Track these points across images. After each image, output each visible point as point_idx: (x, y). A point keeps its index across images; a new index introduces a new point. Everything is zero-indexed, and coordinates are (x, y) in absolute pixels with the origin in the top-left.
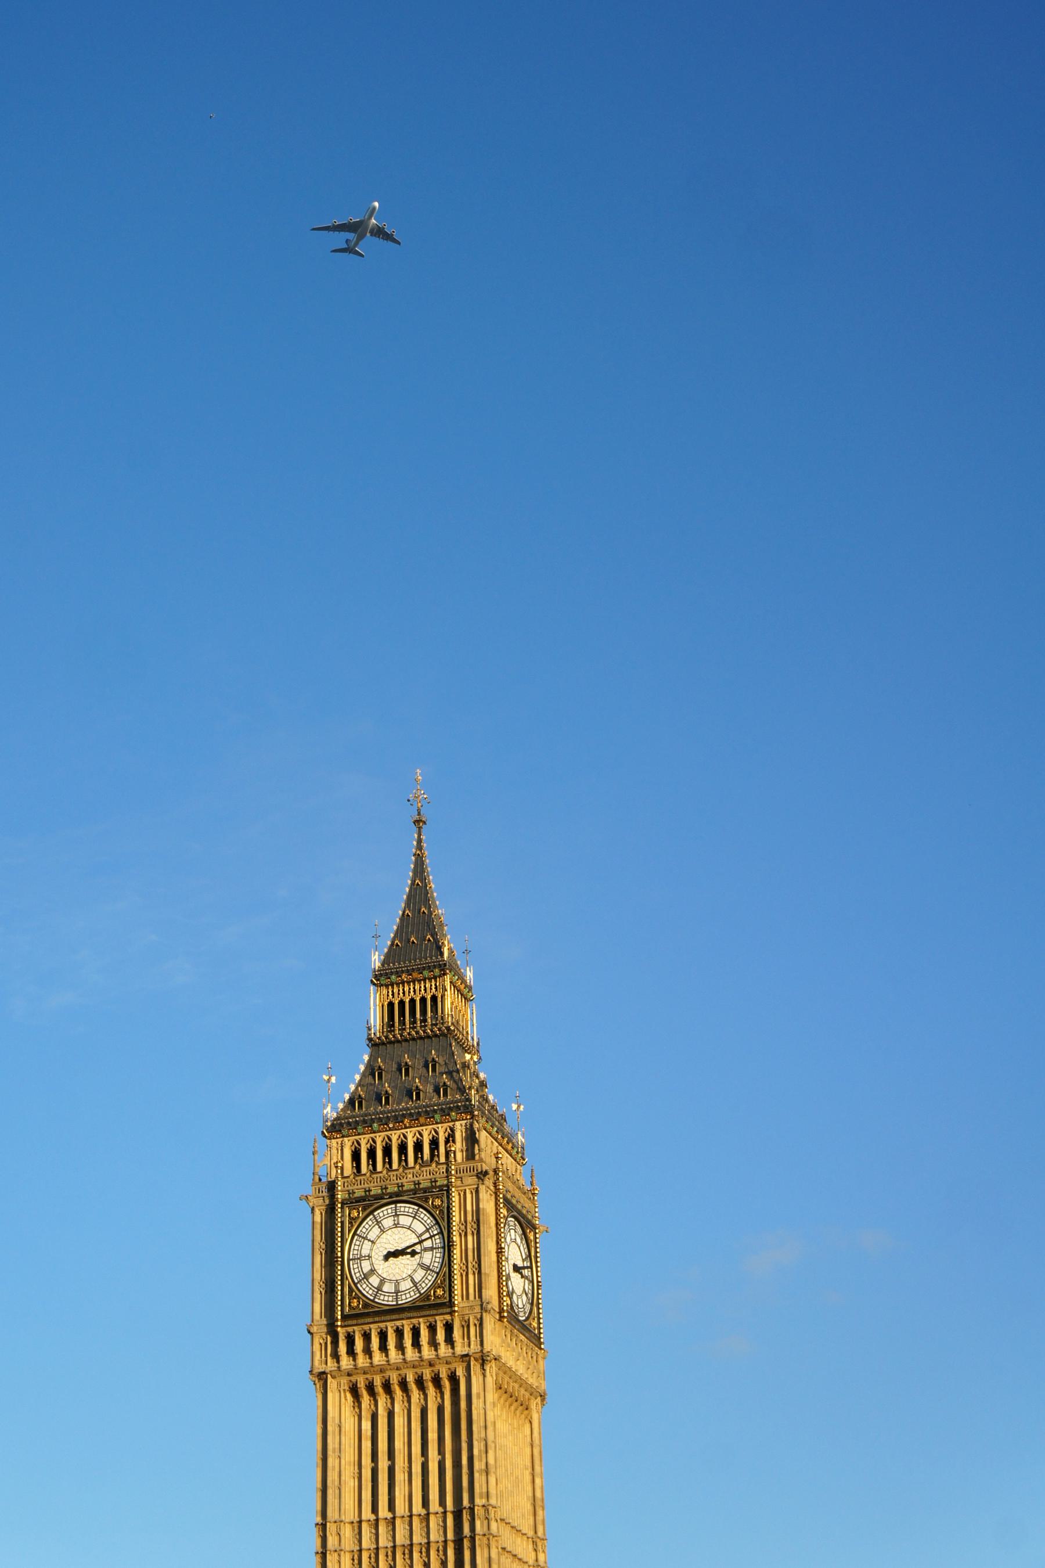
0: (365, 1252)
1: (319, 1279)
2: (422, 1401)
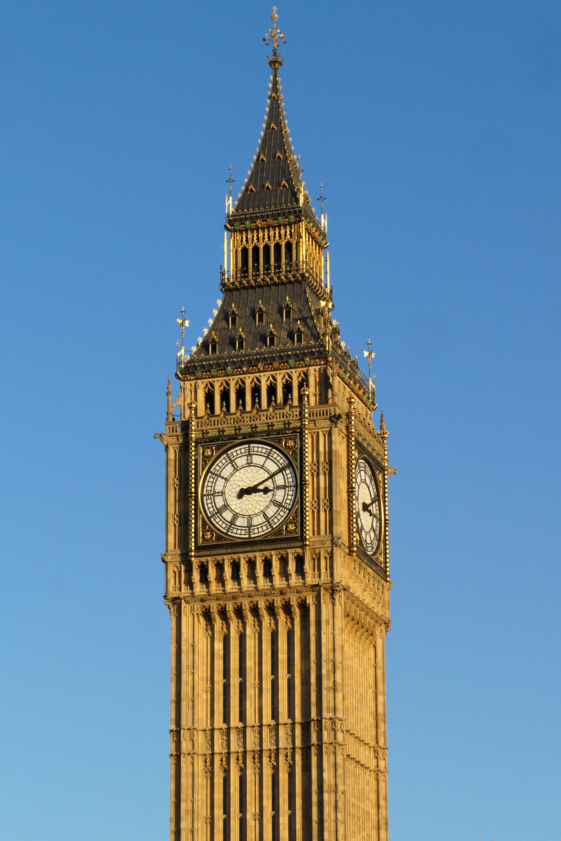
0: (219, 488)
1: (173, 512)
2: (273, 625)
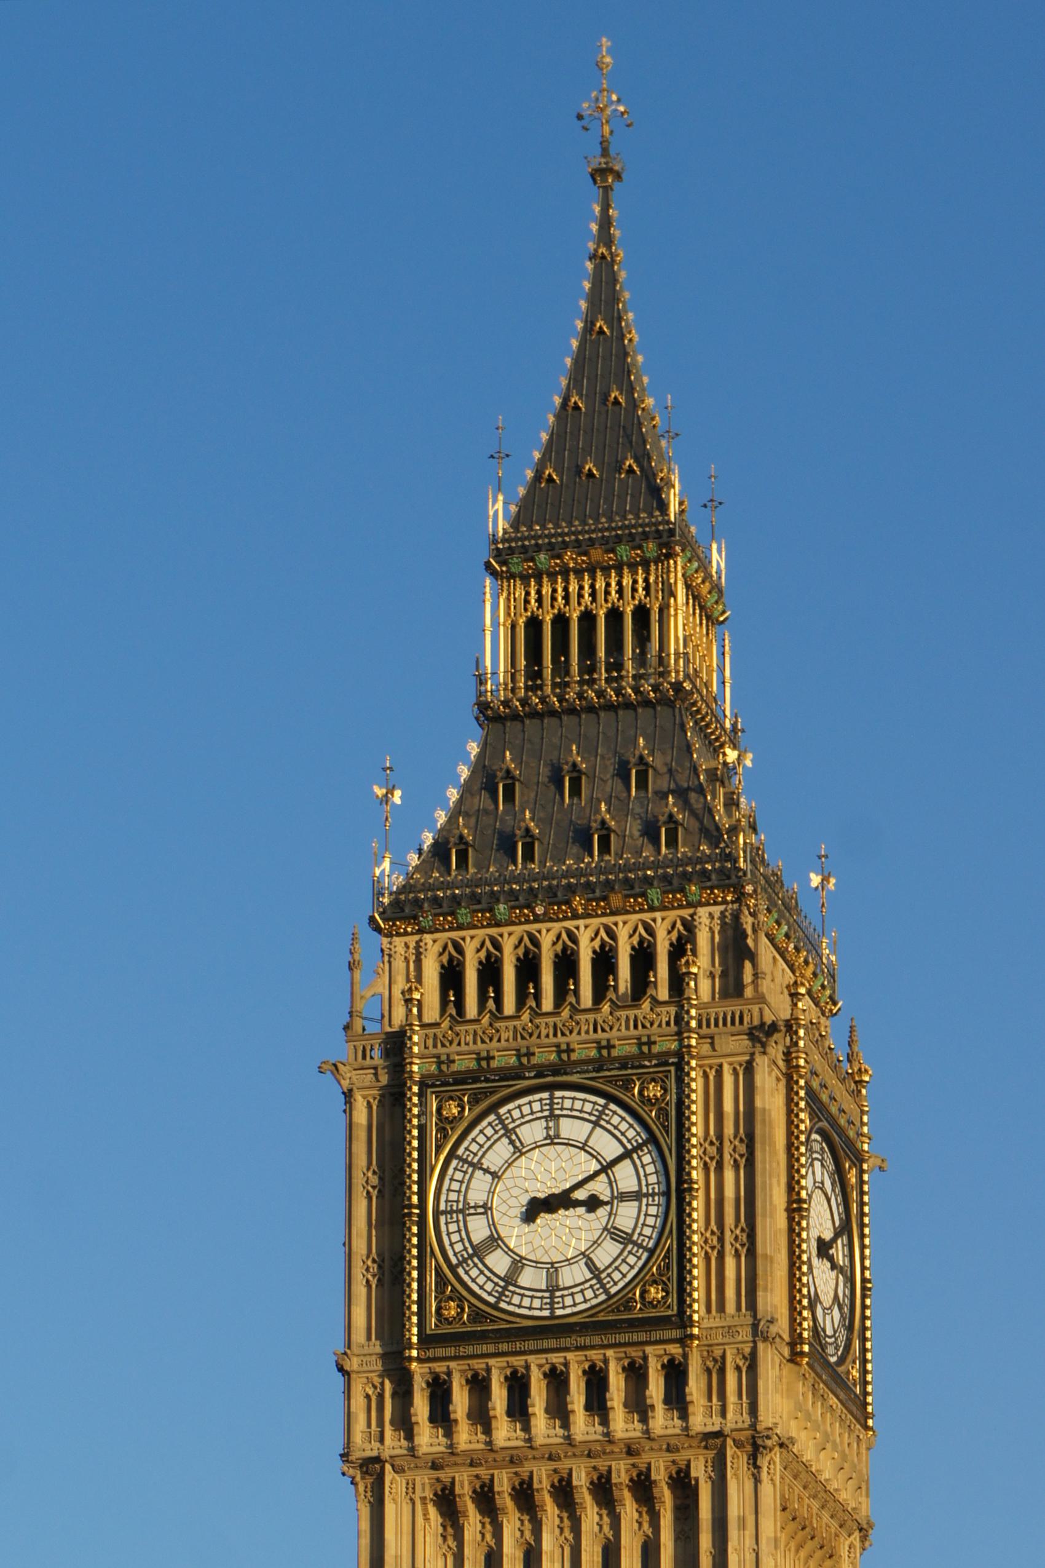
1: (364, 1252)
2: (606, 1529)
